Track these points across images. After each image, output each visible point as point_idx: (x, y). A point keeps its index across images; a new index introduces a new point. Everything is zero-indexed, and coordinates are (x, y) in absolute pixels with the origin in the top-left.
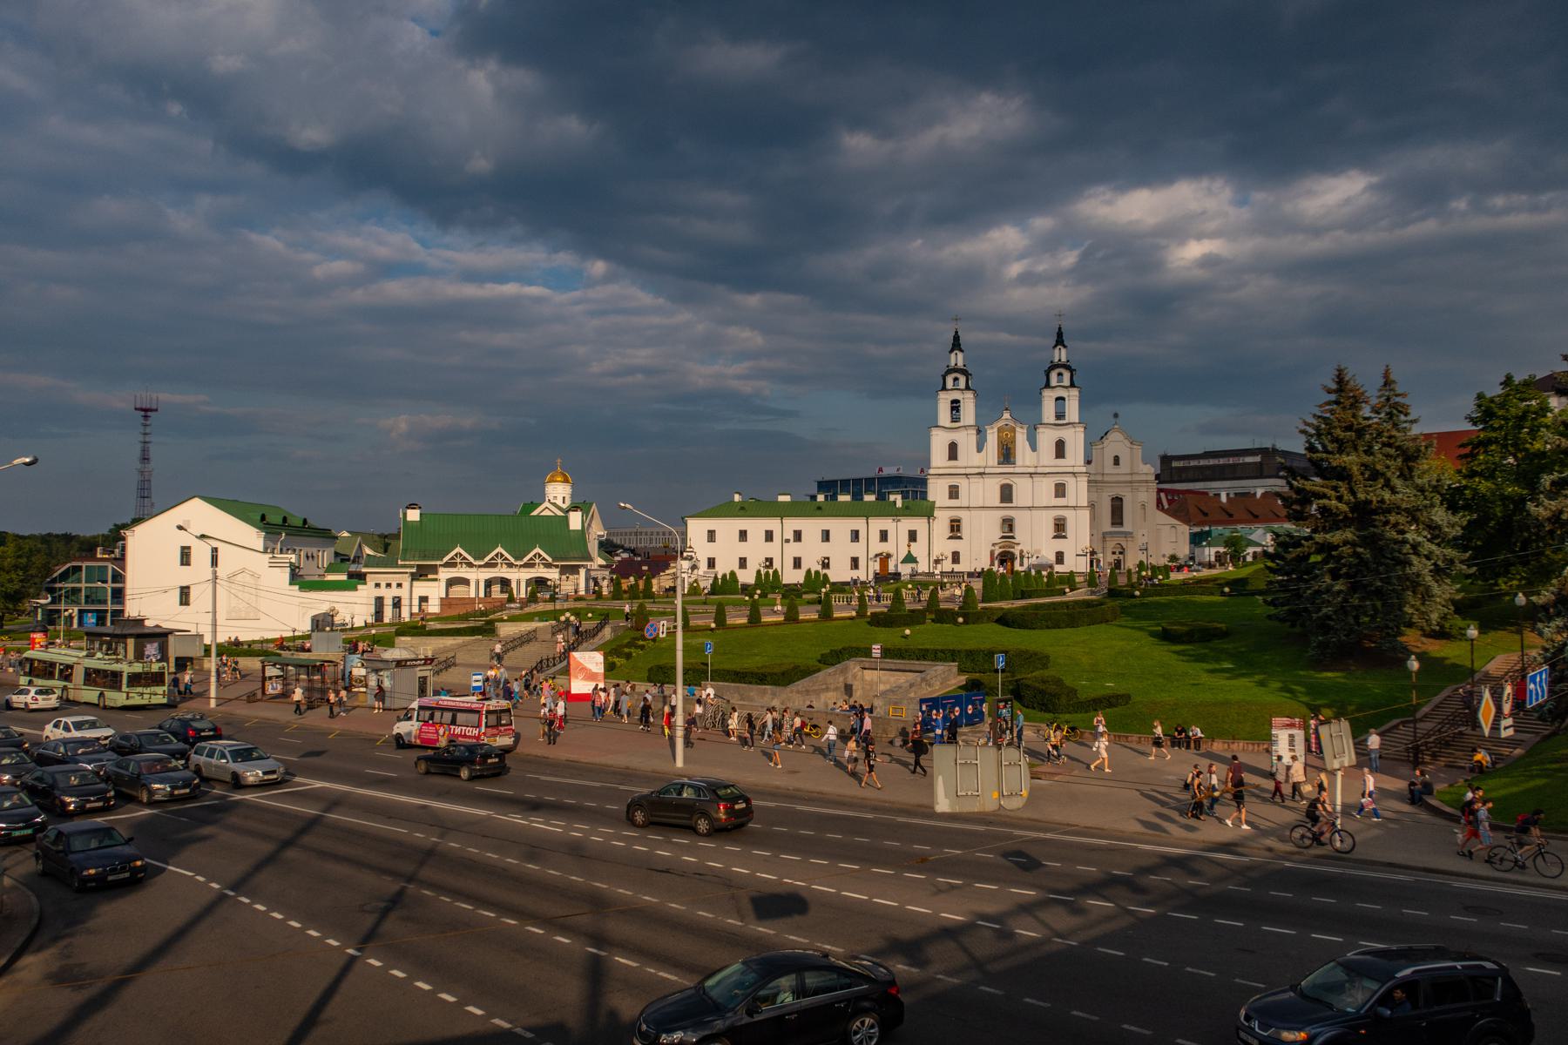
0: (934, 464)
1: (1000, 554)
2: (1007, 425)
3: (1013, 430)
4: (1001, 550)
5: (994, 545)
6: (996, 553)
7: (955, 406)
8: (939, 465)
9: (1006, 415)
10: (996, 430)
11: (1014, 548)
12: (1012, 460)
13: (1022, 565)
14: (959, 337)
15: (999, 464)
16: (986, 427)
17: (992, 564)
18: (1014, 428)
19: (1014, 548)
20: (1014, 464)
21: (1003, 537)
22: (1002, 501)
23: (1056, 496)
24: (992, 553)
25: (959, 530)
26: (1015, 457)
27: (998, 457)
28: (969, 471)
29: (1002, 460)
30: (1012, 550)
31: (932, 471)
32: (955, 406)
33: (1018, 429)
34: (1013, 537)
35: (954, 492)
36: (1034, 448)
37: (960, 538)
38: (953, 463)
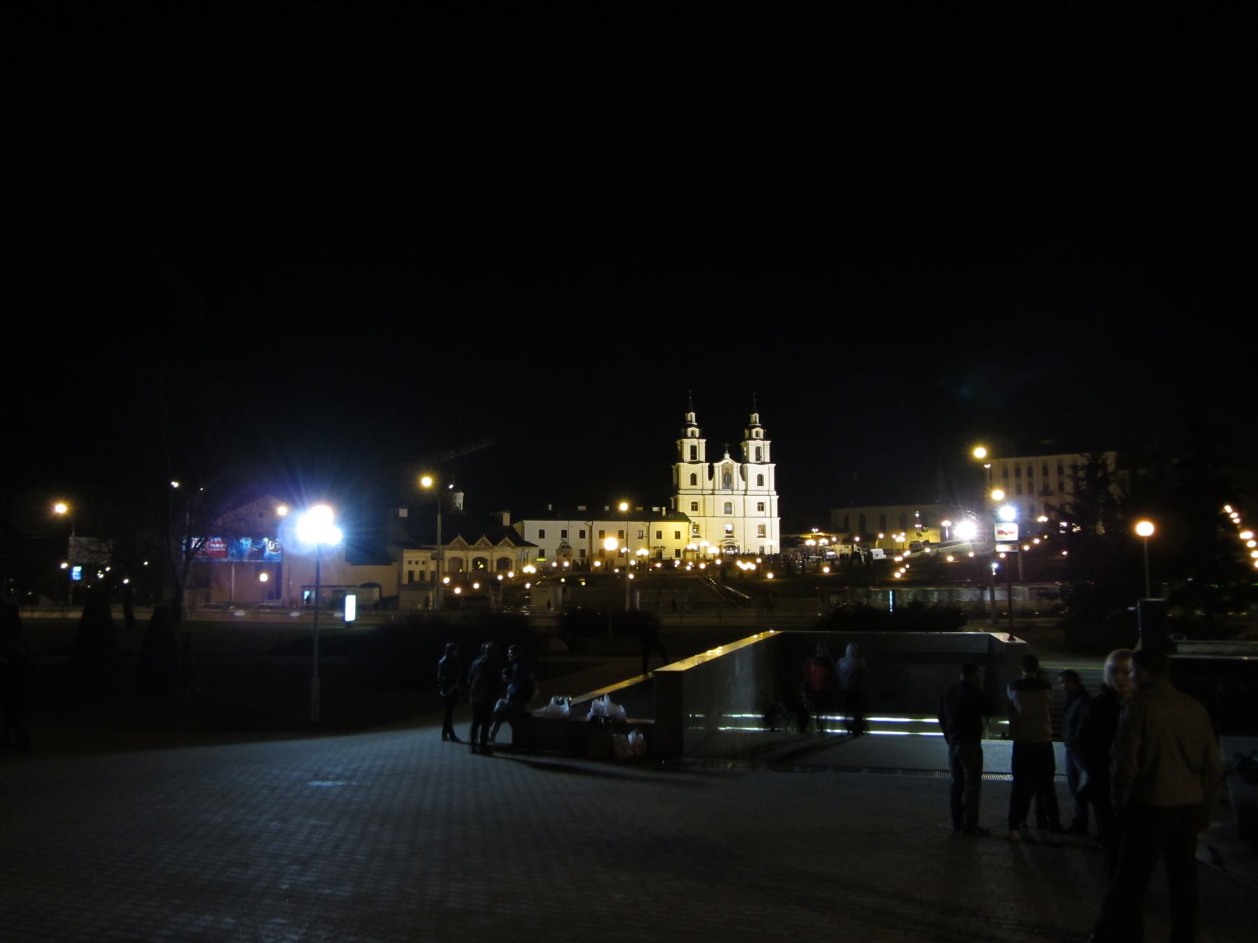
3: (732, 466)
7: (694, 450)
8: (685, 487)
9: (727, 456)
12: (731, 486)
21: (727, 537)
22: (726, 512)
28: (705, 492)
29: (725, 485)
32: (693, 449)
35: (695, 507)
37: (699, 537)
38: (694, 487)
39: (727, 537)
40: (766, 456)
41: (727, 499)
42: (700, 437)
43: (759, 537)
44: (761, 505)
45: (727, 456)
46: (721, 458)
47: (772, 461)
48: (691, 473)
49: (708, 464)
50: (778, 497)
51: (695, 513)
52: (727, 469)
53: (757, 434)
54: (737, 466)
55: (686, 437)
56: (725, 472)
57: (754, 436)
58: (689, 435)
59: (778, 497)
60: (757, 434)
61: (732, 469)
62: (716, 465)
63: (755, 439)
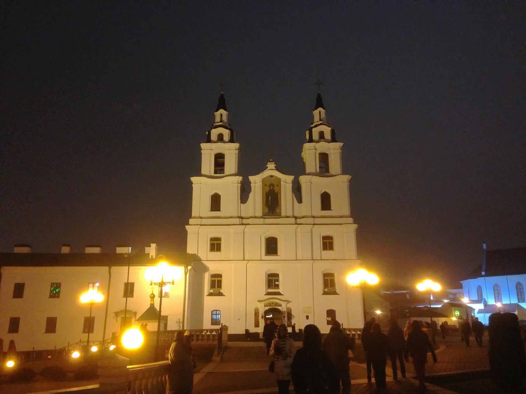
0: (194, 213)
1: (267, 313)
2: (271, 176)
4: (267, 308)
5: (259, 301)
6: (261, 312)
9: (271, 166)
11: (281, 306)
12: (277, 210)
14: (224, 100)
15: (263, 215)
17: (257, 325)
19: (281, 306)
20: (280, 215)
24: (256, 314)
25: (220, 286)
29: (267, 210)
31: (191, 221)
34: (279, 294)
36: (300, 201)
39: (268, 294)
40: (335, 164)
41: (272, 231)
42: (232, 141)
43: (325, 293)
45: (271, 166)
46: (260, 169)
47: (344, 173)
48: (213, 193)
49: (240, 178)
50: (355, 226)
51: (215, 255)
52: (272, 185)
53: (322, 135)
54: (287, 180)
55: (209, 140)
56: (268, 189)
57: (316, 136)
58: (214, 137)
59: (355, 226)
60: (322, 135)
61: (279, 185)
62: (251, 178)
63: (318, 142)
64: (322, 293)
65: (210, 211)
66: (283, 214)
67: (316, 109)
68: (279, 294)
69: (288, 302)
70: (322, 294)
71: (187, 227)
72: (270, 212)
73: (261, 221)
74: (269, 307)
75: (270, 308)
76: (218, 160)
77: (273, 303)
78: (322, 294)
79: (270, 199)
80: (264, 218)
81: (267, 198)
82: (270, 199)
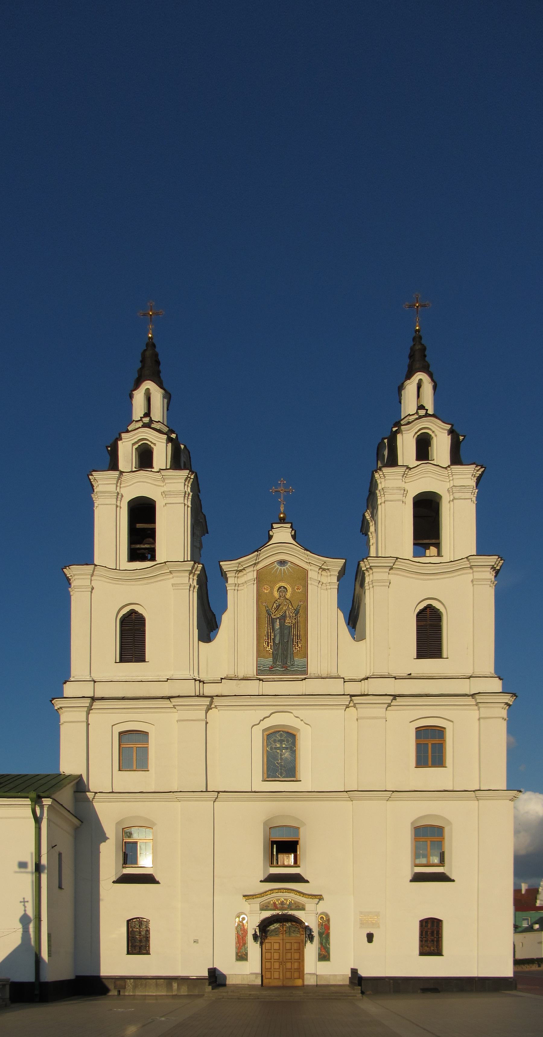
1: (264, 926)
2: (282, 563)
4: (267, 914)
10: (251, 575)
11: (303, 909)
13: (324, 956)
15: (260, 671)
16: (226, 565)
17: (242, 956)
18: (306, 572)
20: (305, 672)
23: (421, 762)
26: (306, 656)
27: (260, 653)
30: (298, 914)
33: (313, 574)
34: (298, 878)
43: (418, 878)
44: (430, 742)
64: (410, 877)
65: (118, 661)
66: (312, 669)
67: (409, 376)
68: (298, 878)
69: (320, 898)
70: (411, 881)
71: (58, 703)
72: (278, 663)
73: (253, 687)
74: (274, 912)
75: (273, 916)
76: (139, 526)
77: (282, 903)
78: (411, 881)
79: (277, 626)
80: (260, 680)
81: (272, 622)
82: (277, 626)
